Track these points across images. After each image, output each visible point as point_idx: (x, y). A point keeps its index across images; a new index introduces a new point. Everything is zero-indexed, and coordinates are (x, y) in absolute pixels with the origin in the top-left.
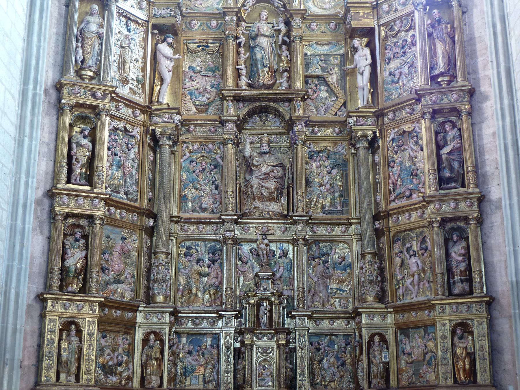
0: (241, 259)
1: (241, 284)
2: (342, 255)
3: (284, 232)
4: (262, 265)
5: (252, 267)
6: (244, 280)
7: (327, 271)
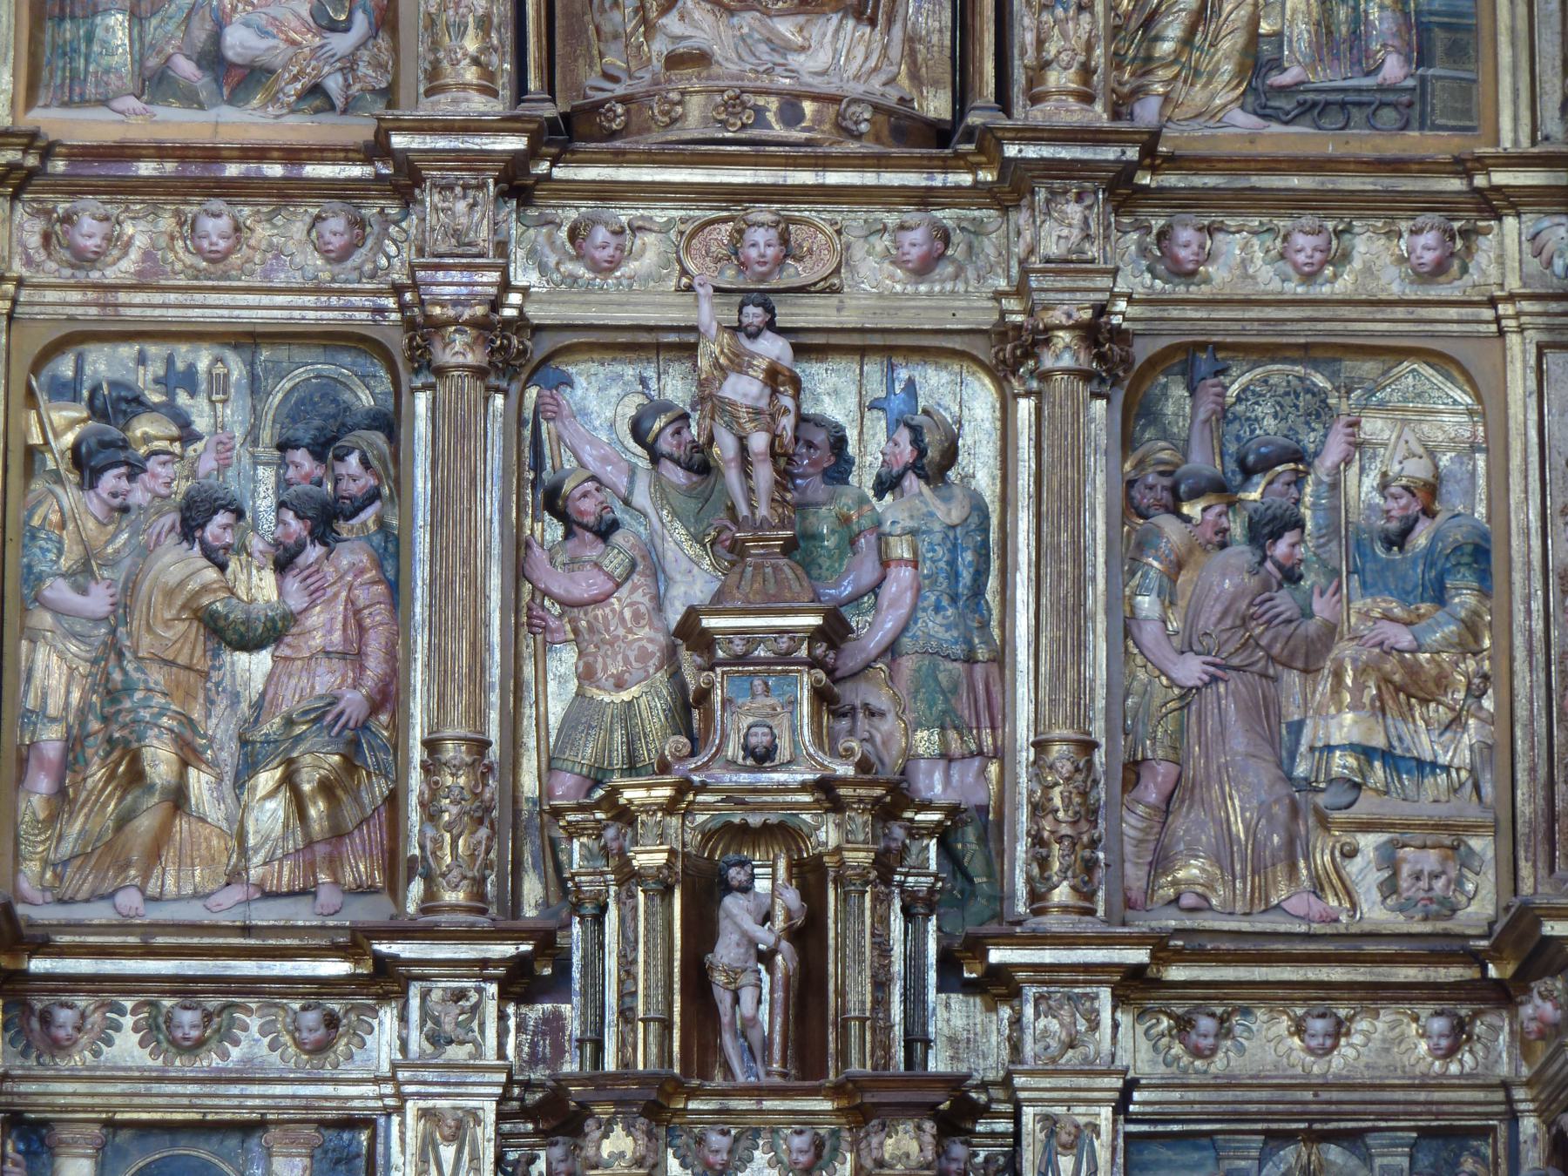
0: (553, 502)
1: (556, 711)
2: (1418, 469)
3: (924, 269)
4: (738, 550)
5: (650, 564)
6: (587, 675)
7: (1284, 601)
